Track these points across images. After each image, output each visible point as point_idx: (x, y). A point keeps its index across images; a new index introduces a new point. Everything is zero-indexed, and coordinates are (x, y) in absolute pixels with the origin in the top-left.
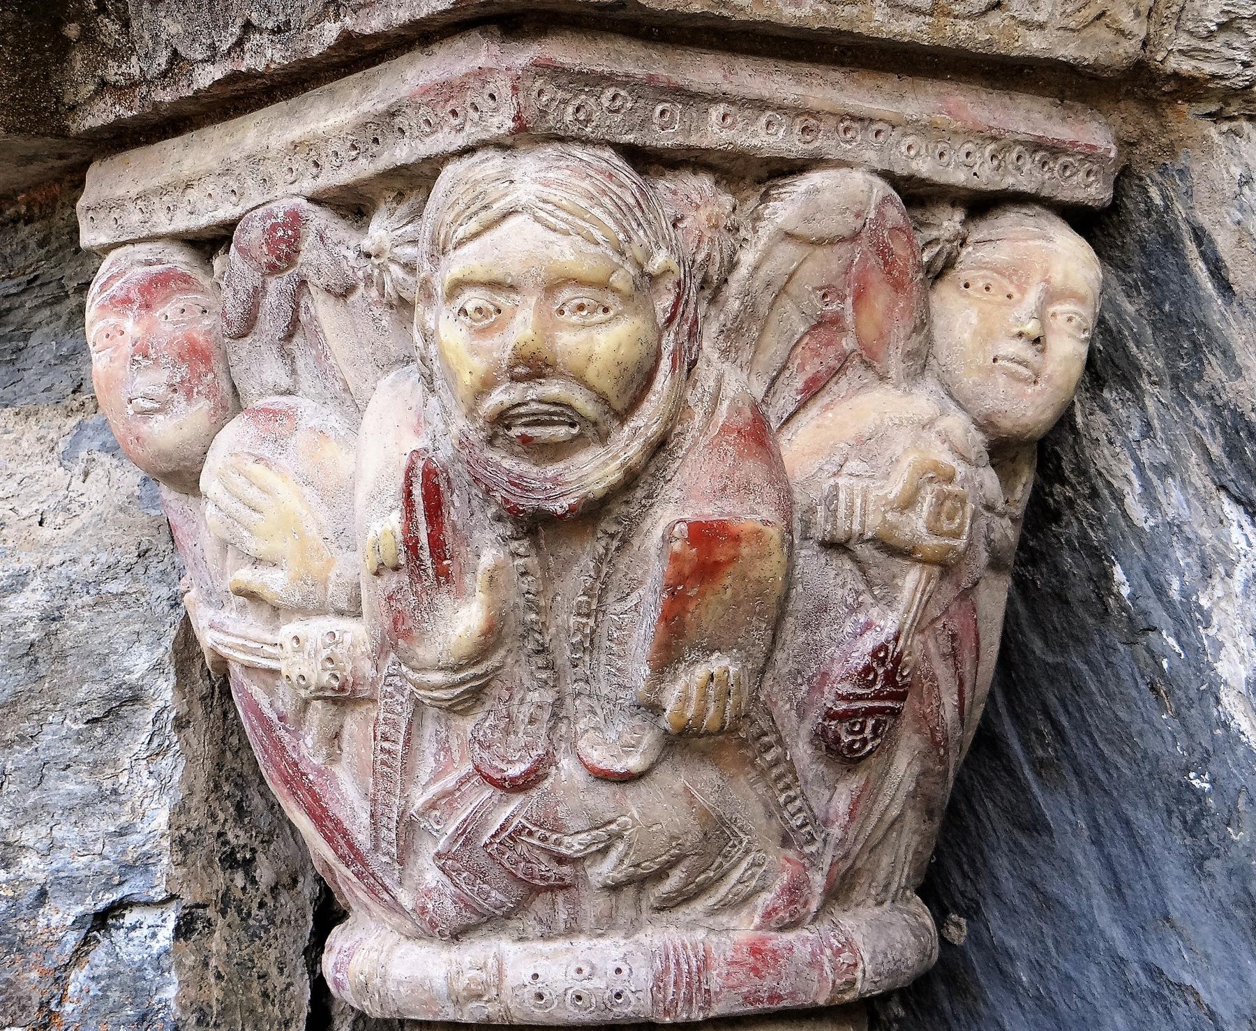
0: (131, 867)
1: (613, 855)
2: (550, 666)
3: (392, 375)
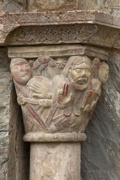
0: (3, 127)
1: (74, 124)
2: (73, 105)
3: (58, 75)
